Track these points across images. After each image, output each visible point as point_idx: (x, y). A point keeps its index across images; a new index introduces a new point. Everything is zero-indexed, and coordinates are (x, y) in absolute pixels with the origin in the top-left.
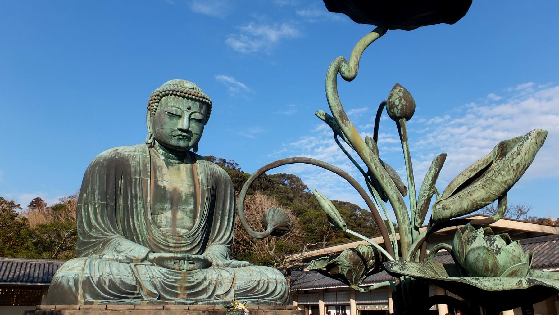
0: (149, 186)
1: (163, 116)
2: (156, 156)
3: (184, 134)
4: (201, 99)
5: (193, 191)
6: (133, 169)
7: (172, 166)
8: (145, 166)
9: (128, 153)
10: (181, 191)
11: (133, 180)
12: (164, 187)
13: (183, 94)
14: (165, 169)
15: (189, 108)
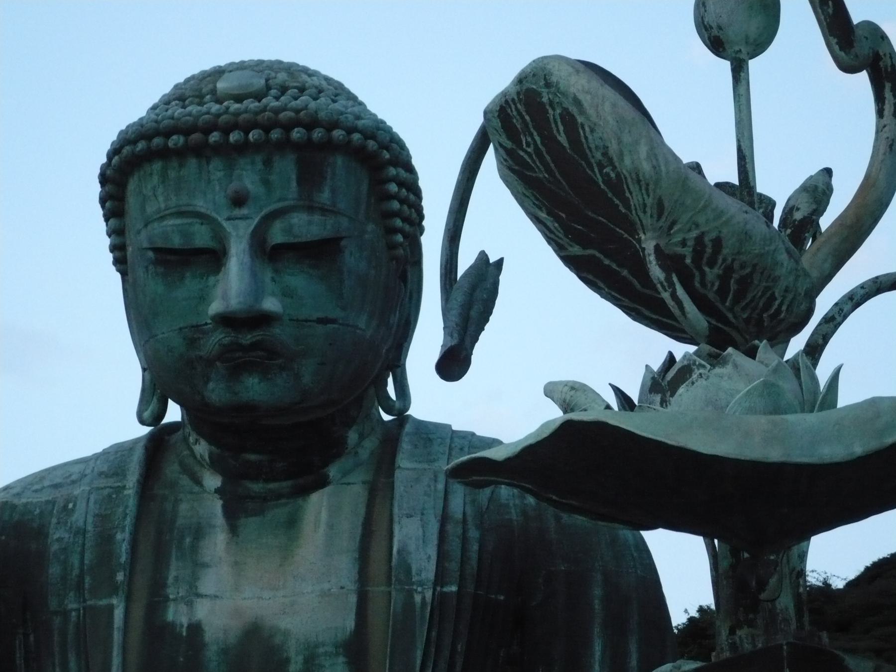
0: (117, 637)
1: (140, 272)
2: (185, 481)
3: (247, 338)
4: (297, 134)
5: (350, 623)
6: (54, 570)
7: (259, 512)
8: (106, 540)
9: (44, 497)
10: (287, 633)
11: (57, 621)
12: (196, 629)
13: (196, 137)
14: (218, 542)
15: (239, 200)
